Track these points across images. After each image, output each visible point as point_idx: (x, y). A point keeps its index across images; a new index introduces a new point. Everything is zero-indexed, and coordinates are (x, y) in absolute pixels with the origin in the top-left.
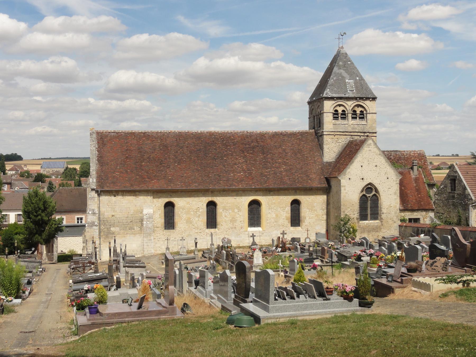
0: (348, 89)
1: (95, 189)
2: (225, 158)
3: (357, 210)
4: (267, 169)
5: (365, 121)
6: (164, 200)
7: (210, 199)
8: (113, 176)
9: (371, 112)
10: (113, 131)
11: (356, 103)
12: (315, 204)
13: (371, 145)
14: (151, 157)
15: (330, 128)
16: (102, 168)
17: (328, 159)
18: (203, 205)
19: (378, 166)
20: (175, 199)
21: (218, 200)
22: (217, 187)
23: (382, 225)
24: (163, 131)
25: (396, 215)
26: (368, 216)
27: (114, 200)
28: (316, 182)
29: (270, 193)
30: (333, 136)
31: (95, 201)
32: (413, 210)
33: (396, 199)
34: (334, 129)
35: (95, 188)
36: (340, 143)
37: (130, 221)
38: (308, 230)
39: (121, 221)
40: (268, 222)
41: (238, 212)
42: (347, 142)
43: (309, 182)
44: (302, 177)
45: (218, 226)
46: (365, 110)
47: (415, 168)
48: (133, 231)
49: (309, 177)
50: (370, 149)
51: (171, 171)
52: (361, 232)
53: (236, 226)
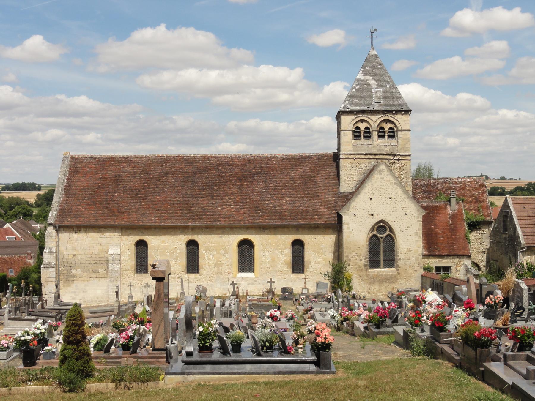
0: (374, 100)
1: (52, 224)
2: (216, 188)
3: (364, 254)
4: (264, 201)
5: (396, 141)
6: (135, 238)
7: (190, 237)
8: (78, 209)
9: (403, 129)
10: (90, 156)
11: (384, 118)
12: (323, 246)
14: (128, 186)
15: (349, 149)
16: (67, 199)
17: (345, 189)
18: (181, 244)
19: (393, 198)
20: (147, 236)
21: (200, 239)
22: (197, 223)
23: (399, 274)
24: (148, 156)
25: (418, 262)
26: (380, 262)
28: (324, 218)
30: (353, 159)
31: (53, 237)
32: (441, 256)
34: (354, 151)
35: (53, 223)
36: (361, 168)
37: (94, 262)
38: (305, 279)
41: (225, 253)
43: (315, 218)
44: (307, 211)
45: (200, 271)
46: (396, 126)
47: (453, 201)
48: (97, 274)
49: (316, 211)
50: (382, 176)
51: (147, 204)
52: (370, 283)
53: (221, 271)
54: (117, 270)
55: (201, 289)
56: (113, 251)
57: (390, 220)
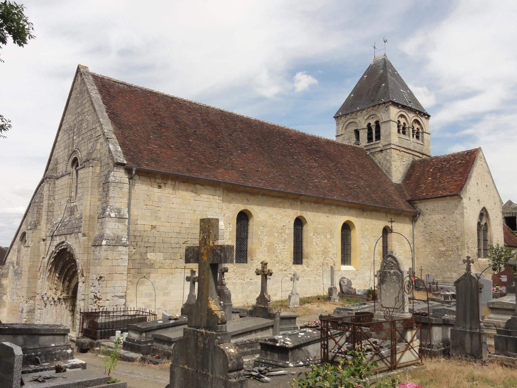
10: (121, 82)
13: (482, 158)
16: (122, 132)
17: (395, 180)
20: (253, 206)
24: (197, 103)
27: (157, 195)
29: (363, 214)
31: (124, 190)
33: (501, 231)
35: (125, 162)
37: (183, 241)
39: (168, 240)
40: (361, 257)
41: (331, 238)
42: (410, 162)
45: (304, 260)
46: (422, 128)
53: (327, 261)
55: (346, 283)
57: (488, 208)
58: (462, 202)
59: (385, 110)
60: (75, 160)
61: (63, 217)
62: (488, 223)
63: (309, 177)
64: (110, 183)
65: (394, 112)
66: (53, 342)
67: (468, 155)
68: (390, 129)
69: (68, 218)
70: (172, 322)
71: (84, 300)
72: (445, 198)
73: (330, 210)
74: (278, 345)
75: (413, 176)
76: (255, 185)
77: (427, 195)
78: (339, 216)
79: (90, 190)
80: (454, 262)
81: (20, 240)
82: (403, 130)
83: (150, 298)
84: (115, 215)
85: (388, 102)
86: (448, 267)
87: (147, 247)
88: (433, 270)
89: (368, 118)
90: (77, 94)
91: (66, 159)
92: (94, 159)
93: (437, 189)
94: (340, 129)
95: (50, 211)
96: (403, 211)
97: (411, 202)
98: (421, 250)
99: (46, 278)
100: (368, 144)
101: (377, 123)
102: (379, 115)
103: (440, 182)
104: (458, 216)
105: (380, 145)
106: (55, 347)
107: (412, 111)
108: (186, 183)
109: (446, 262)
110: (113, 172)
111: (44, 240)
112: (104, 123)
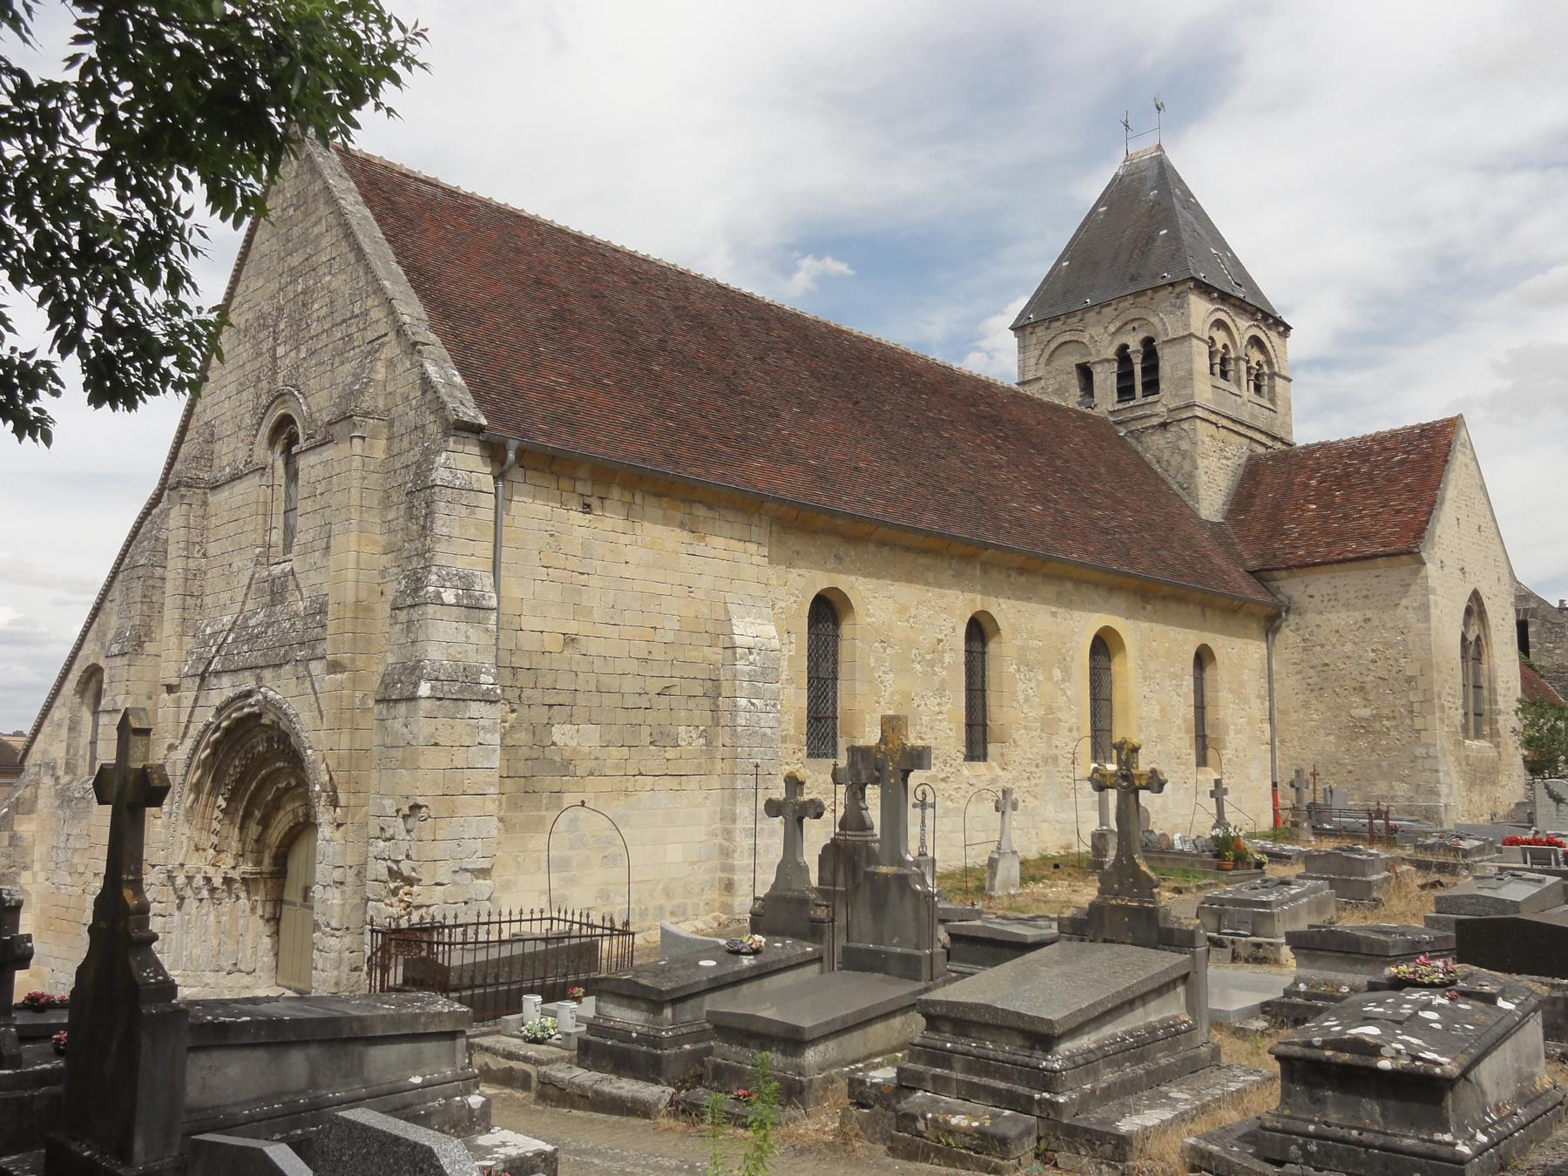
1: (479, 429)
17: (1207, 512)
20: (853, 578)
29: (1144, 608)
31: (480, 513)
35: (484, 422)
36: (1228, 459)
37: (657, 685)
42: (1243, 460)
45: (992, 748)
46: (1270, 363)
48: (671, 753)
53: (1056, 752)
54: (769, 731)
56: (751, 631)
57: (1484, 593)
58: (1423, 574)
59: (1175, 306)
60: (286, 421)
61: (241, 612)
62: (1482, 636)
63: (994, 495)
64: (437, 489)
65: (1200, 310)
66: (416, 1068)
67: (1426, 437)
68: (1191, 361)
69: (262, 614)
70: (747, 961)
71: (342, 883)
72: (1367, 564)
73: (1059, 594)
74: (1384, 1064)
75: (1257, 501)
76: (859, 510)
77: (1309, 554)
78: (1083, 614)
79: (355, 515)
80: (1399, 750)
81: (76, 692)
82: (1222, 366)
83: (565, 874)
84: (457, 595)
85: (1185, 281)
86: (1379, 766)
87: (551, 706)
88: (1333, 774)
89: (1119, 330)
90: (284, 210)
91: (248, 421)
92: (366, 414)
93: (1341, 536)
94: (1033, 361)
95: (192, 594)
96: (1246, 601)
97: (1260, 576)
98: (1294, 716)
99: (181, 812)
100: (1120, 406)
101: (1148, 343)
102: (1154, 320)
103: (1346, 517)
104: (1411, 616)
105: (1159, 409)
106: (422, 1086)
107: (1245, 310)
108: (665, 499)
109: (1373, 751)
110: (444, 454)
111: (170, 689)
112: (398, 295)
